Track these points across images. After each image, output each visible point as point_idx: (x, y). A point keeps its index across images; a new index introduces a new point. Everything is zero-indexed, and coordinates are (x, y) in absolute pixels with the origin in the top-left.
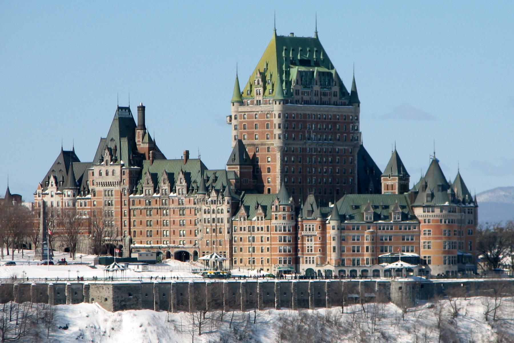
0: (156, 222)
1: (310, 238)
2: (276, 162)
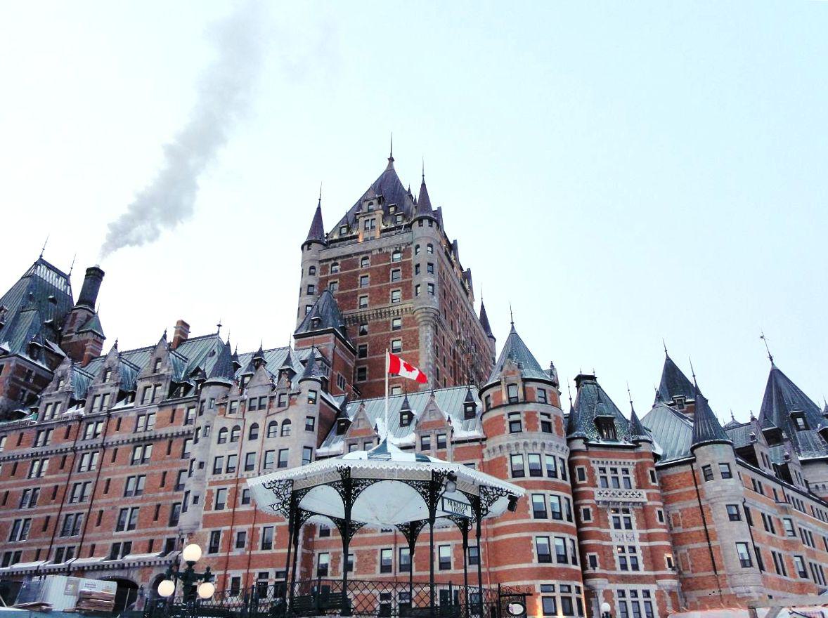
0: (53, 489)
1: (621, 515)
2: (417, 347)
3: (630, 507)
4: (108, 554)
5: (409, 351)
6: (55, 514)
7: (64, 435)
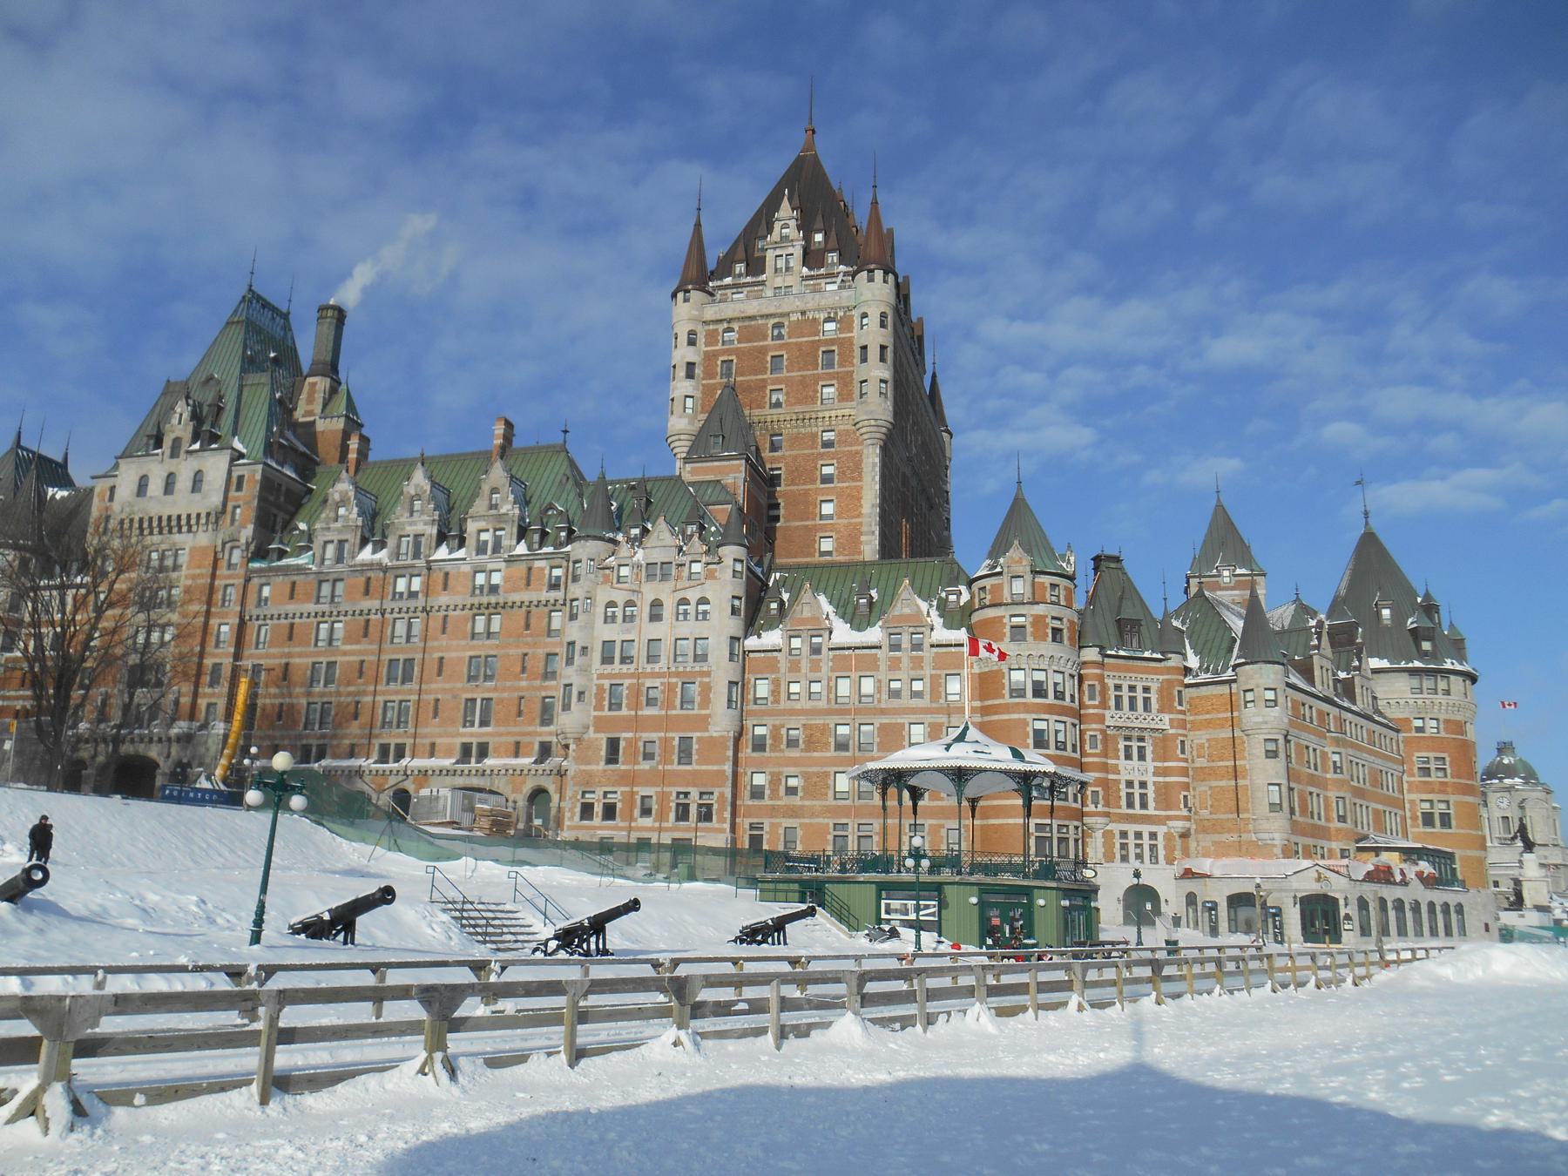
1: (1135, 744)
2: (860, 478)
3: (1146, 734)
4: (457, 756)
5: (845, 485)
6: (368, 699)
7: (362, 590)
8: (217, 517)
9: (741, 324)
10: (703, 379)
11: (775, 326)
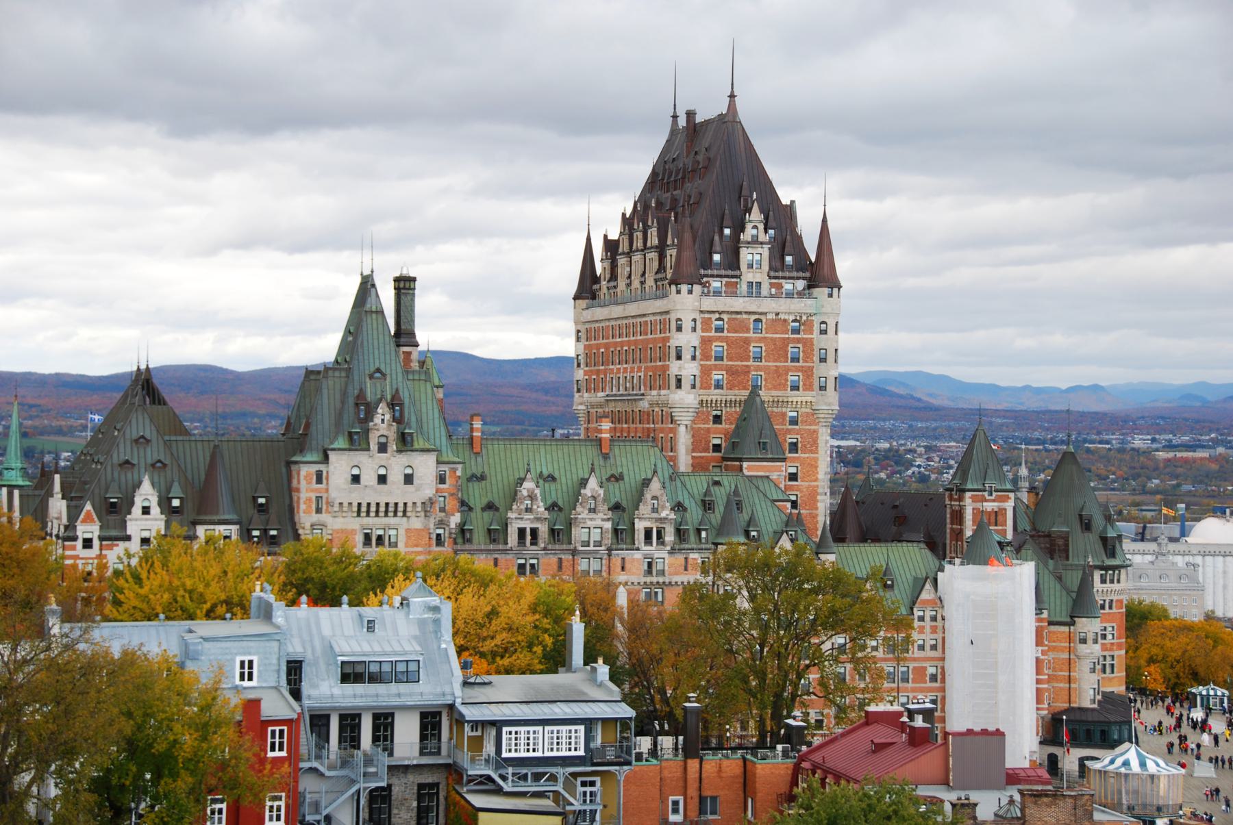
5: (807, 455)
8: (428, 506)
9: (729, 316)
10: (701, 360)
11: (755, 321)
